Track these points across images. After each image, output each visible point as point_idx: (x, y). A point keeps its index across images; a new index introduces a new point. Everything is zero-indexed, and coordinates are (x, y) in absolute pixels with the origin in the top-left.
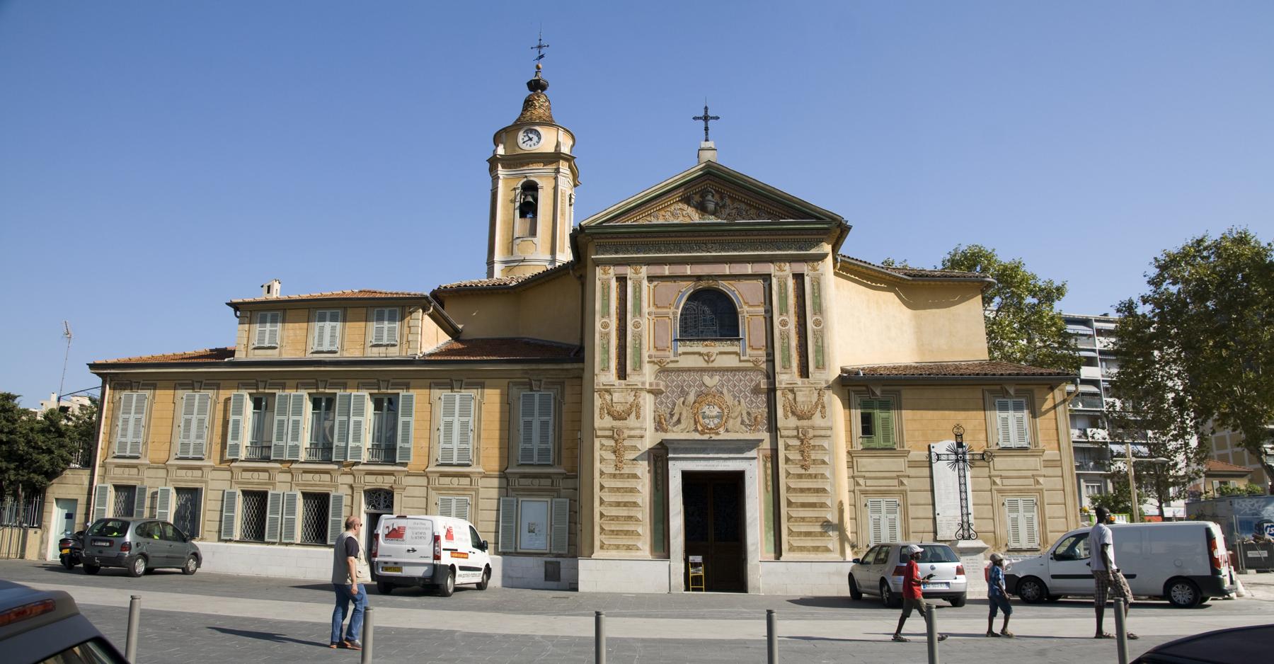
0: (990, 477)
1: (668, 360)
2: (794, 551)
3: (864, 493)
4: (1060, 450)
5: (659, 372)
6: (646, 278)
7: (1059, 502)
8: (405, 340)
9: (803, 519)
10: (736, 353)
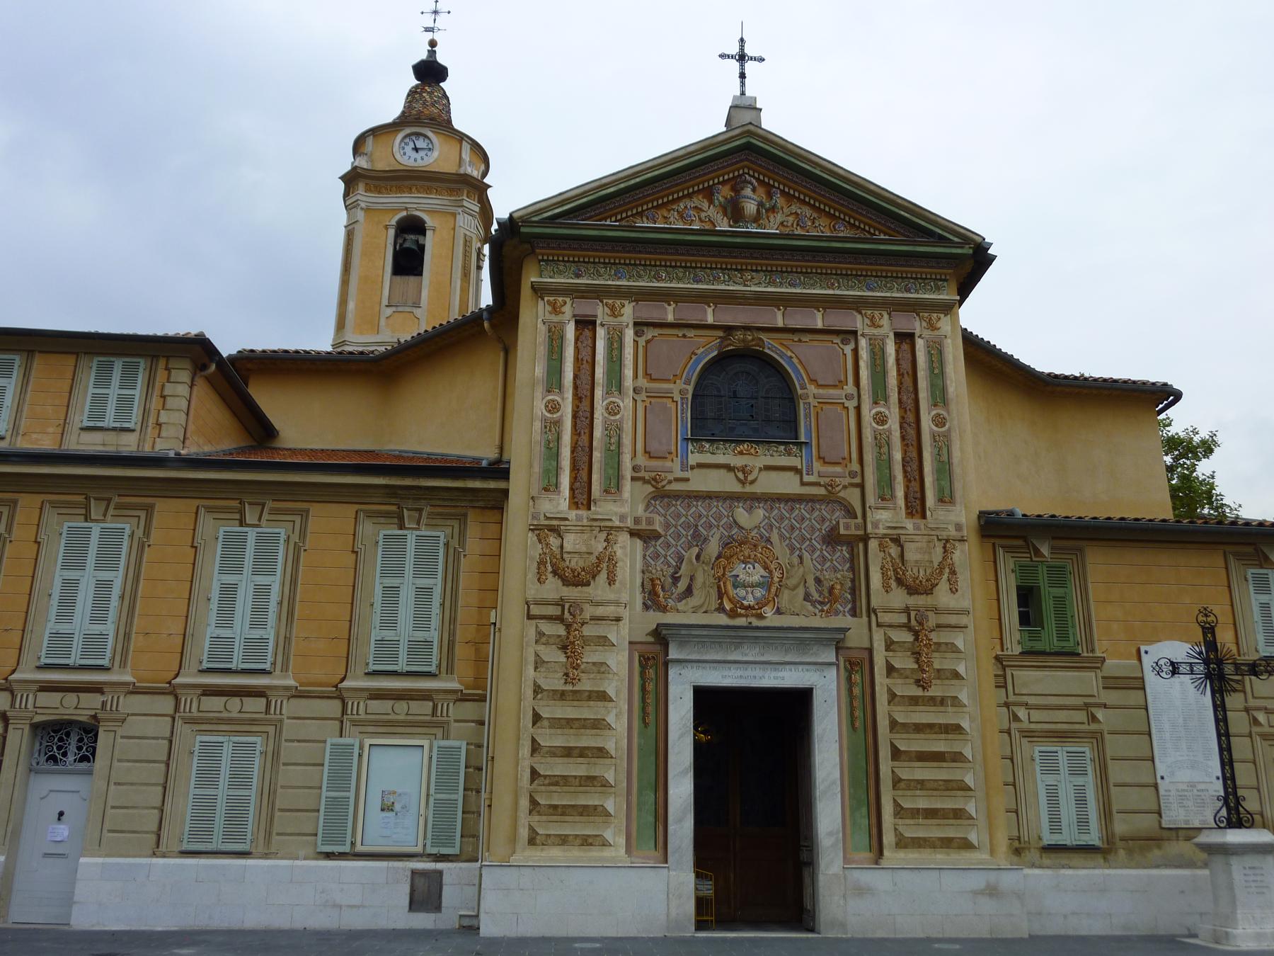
0: (1247, 710)
1: (670, 477)
2: (905, 847)
3: (1028, 734)
6: (631, 325)
8: (152, 420)
9: (921, 784)
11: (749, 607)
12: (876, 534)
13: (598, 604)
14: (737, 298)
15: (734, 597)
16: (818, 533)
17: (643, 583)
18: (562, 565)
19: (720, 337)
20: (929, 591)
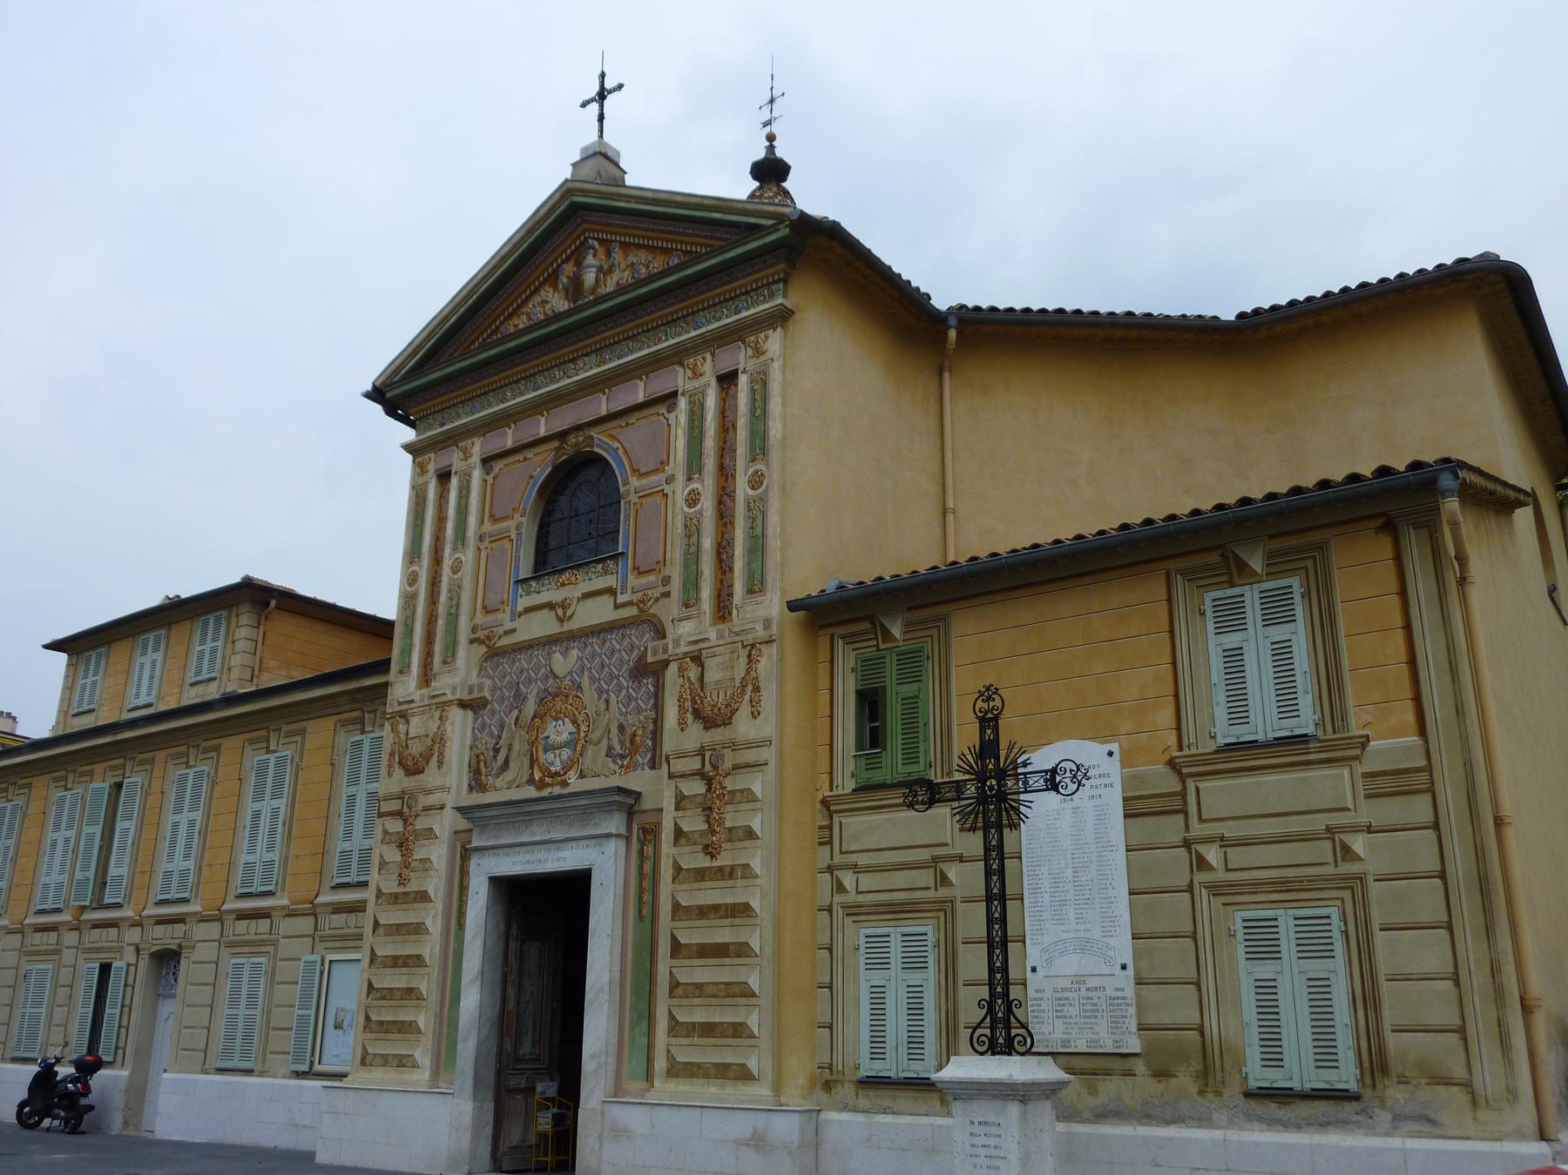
0: (1187, 844)
3: (853, 911)
4: (1422, 731)
5: (486, 660)
7: (1425, 918)
9: (699, 989)
10: (610, 591)
11: (557, 774)
12: (677, 655)
13: (429, 792)
14: (565, 396)
15: (543, 764)
16: (626, 666)
17: (470, 761)
18: (407, 752)
19: (555, 449)
20: (727, 722)
